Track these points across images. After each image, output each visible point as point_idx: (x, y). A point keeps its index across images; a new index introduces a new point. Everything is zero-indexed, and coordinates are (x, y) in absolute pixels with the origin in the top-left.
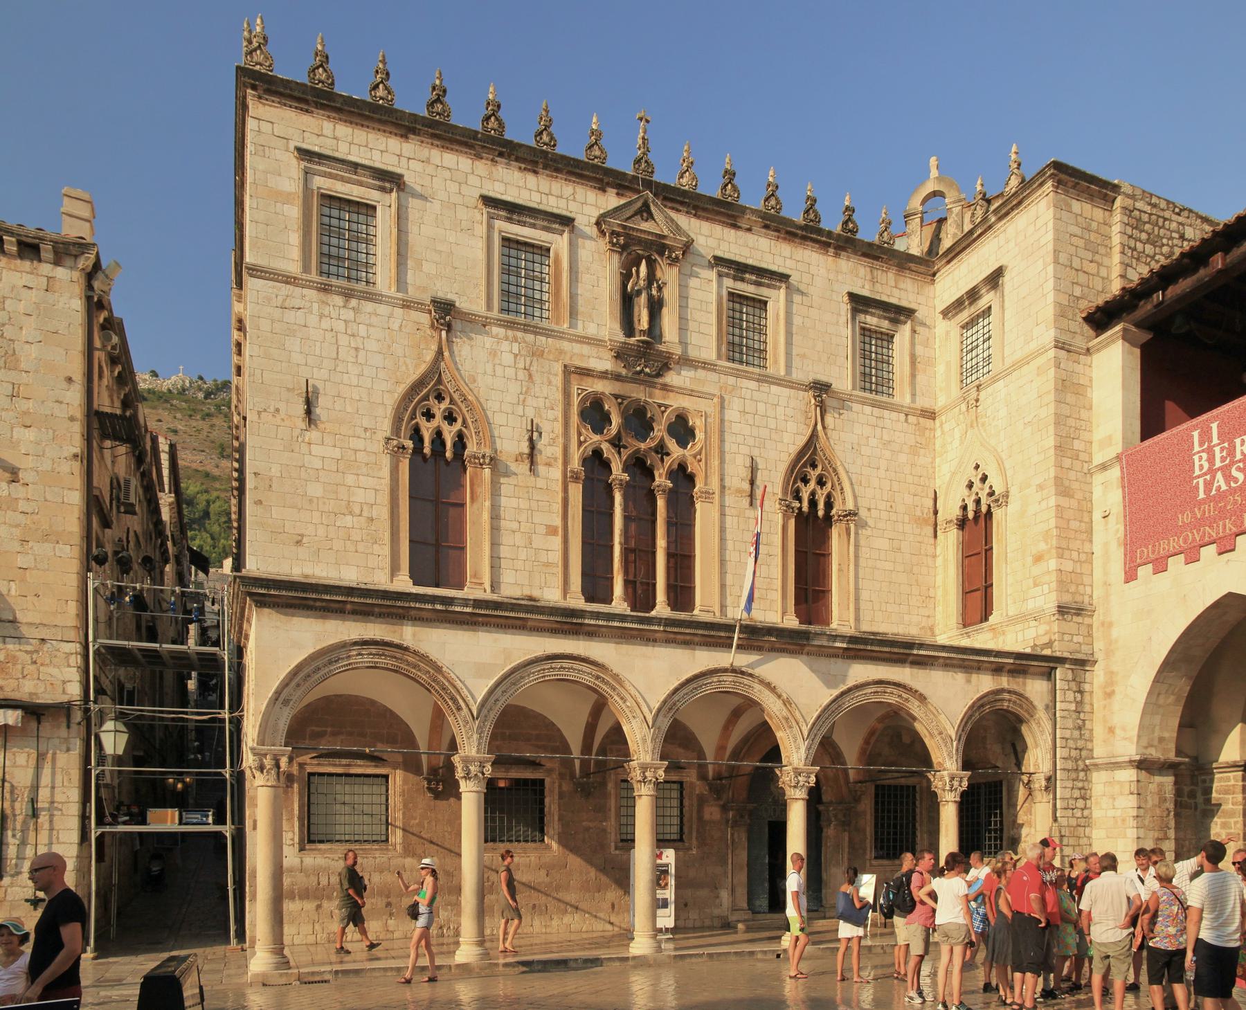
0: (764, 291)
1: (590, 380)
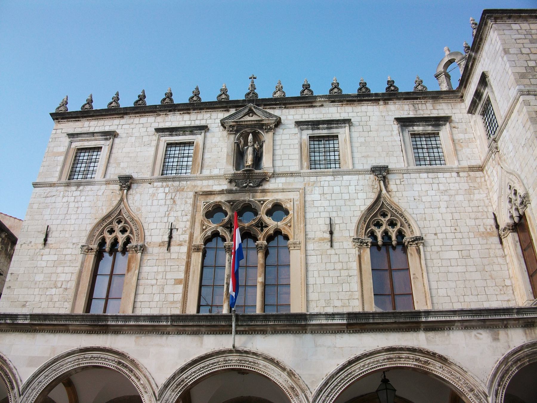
0: (334, 131)
1: (212, 197)
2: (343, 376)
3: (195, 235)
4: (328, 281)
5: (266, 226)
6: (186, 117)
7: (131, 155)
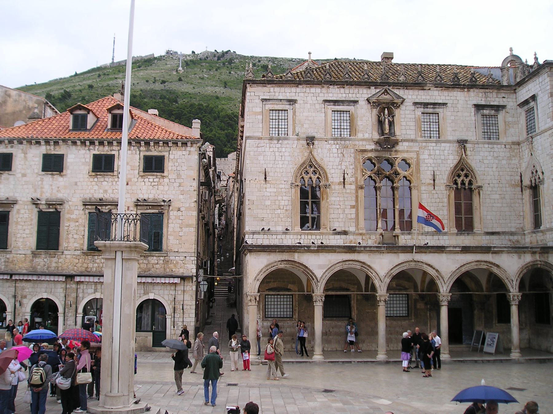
0: (437, 110)
1: (366, 153)
3: (359, 178)
5: (398, 174)
6: (342, 90)
7: (310, 118)
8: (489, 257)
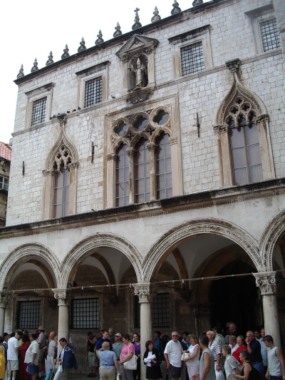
0: (198, 38)
2: (162, 245)
4: (198, 164)
5: (154, 130)
6: (96, 57)
8: (212, 213)
